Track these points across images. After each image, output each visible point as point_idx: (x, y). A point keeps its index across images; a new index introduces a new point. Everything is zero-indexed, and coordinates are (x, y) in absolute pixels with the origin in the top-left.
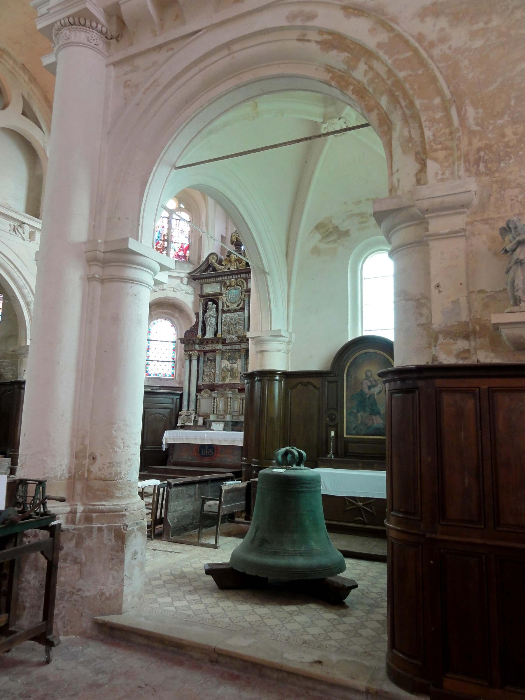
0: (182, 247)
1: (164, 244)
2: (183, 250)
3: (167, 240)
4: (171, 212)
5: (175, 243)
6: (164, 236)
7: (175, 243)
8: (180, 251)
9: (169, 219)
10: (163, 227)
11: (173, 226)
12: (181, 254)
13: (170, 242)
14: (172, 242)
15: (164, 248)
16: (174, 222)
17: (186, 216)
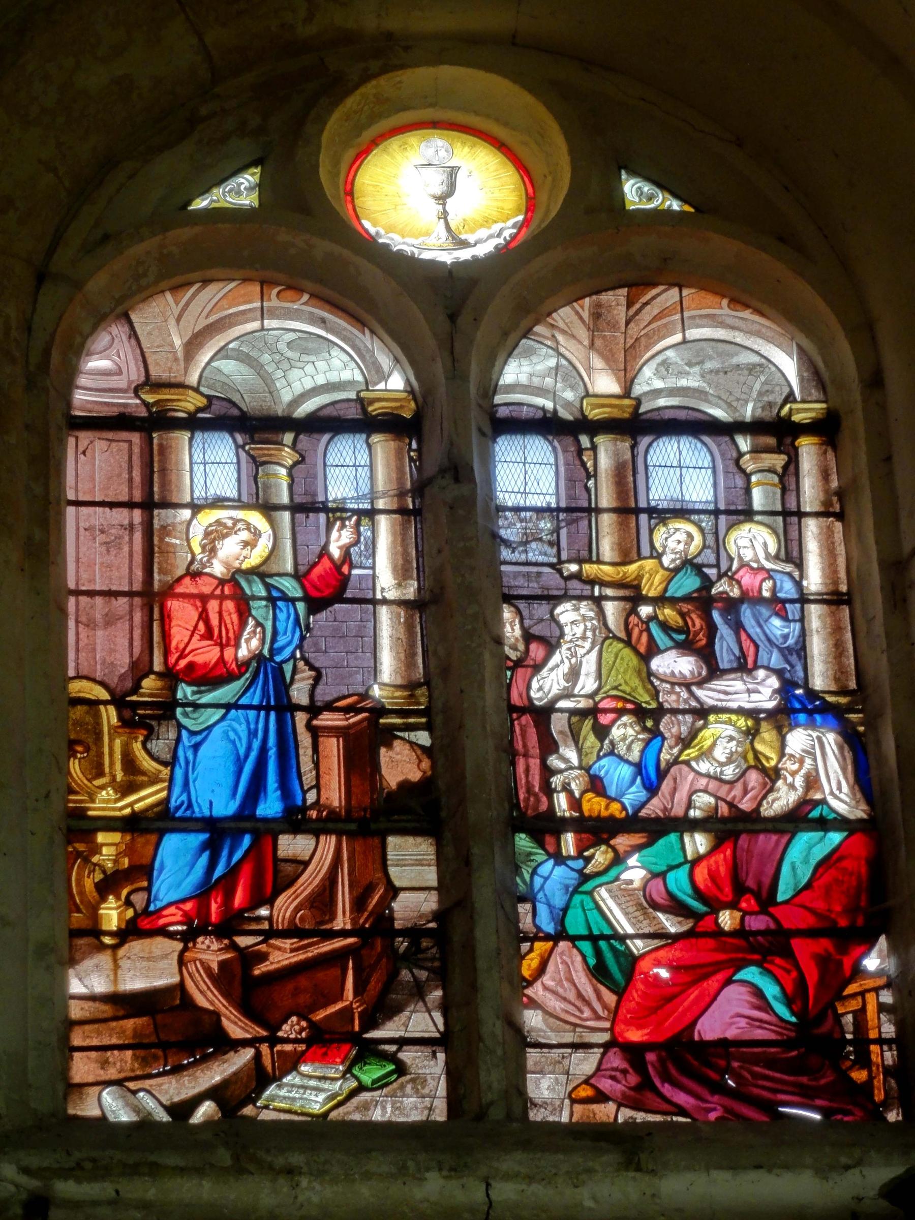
0: (745, 883)
1: (375, 887)
2: (765, 947)
3: (417, 810)
4: (448, 316)
5: (597, 830)
6: (367, 737)
7: (597, 830)
8: (709, 956)
9: (440, 446)
10: (330, 589)
11: (524, 553)
12: (740, 1007)
13: (484, 810)
14: (546, 828)
15: (386, 958)
16: (524, 475)
17: (735, 354)
